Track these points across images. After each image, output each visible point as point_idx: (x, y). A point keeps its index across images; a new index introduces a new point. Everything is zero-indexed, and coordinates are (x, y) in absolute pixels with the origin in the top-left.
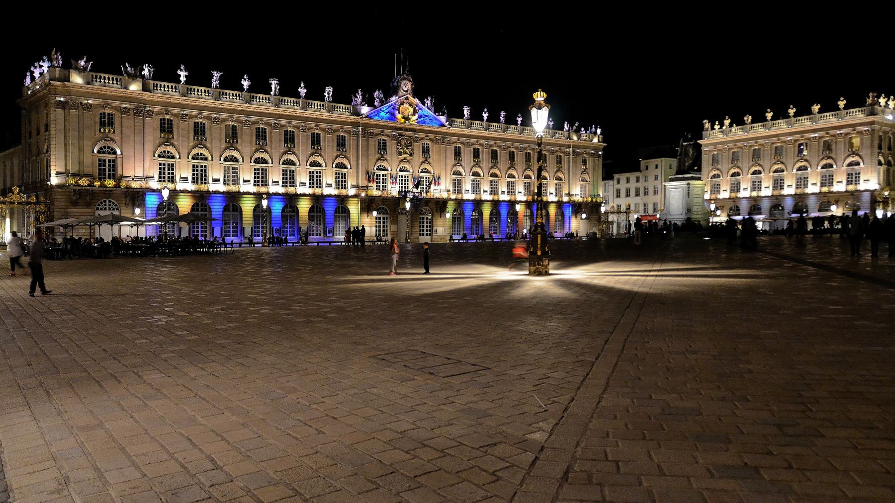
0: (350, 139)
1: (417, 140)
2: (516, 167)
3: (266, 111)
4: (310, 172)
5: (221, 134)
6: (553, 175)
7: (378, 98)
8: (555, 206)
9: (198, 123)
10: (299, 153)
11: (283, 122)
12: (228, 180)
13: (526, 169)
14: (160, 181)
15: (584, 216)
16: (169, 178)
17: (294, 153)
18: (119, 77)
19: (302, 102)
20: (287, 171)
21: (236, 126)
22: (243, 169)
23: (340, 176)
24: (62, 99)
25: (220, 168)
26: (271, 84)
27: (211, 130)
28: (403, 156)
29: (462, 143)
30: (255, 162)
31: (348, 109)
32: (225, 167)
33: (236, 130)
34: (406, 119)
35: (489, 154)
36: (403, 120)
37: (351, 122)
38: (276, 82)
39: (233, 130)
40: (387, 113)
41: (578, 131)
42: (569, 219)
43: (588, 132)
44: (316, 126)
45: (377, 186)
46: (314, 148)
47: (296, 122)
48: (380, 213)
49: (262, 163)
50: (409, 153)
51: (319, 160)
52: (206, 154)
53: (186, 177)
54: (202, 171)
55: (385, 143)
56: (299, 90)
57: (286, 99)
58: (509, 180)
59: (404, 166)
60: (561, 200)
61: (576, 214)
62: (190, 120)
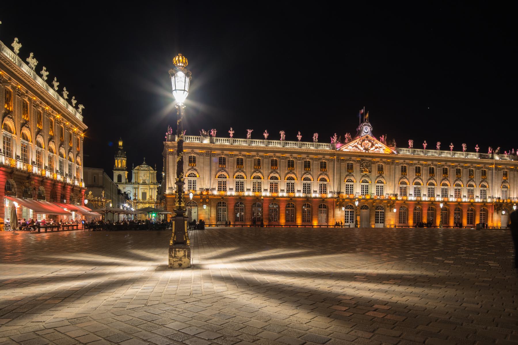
0: (329, 164)
1: (374, 163)
2: (449, 179)
3: (277, 150)
4: (304, 184)
5: (251, 164)
6: (479, 184)
7: (347, 138)
9: (239, 158)
10: (297, 173)
11: (287, 155)
12: (256, 189)
13: (456, 180)
14: (219, 191)
15: (504, 212)
16: (223, 189)
17: (294, 173)
18: (199, 137)
19: (299, 143)
20: (289, 184)
21: (260, 159)
22: (263, 183)
23: (323, 186)
24: (172, 150)
25: (251, 183)
26: (281, 134)
27: (246, 162)
28: (365, 173)
29: (407, 164)
30: (270, 179)
31: (328, 146)
32: (254, 183)
33: (260, 161)
35: (427, 171)
36: (364, 151)
37: (330, 154)
38: (283, 133)
39: (258, 161)
40: (353, 147)
41: (501, 152)
42: (492, 215)
43: (509, 154)
44: (307, 157)
45: (346, 192)
46: (306, 170)
48: (348, 209)
49: (275, 179)
50: (368, 171)
51: (309, 176)
52: (243, 175)
53: (232, 188)
54: (241, 185)
55: (352, 165)
56: (297, 136)
57: (289, 142)
58: (443, 187)
59: (365, 179)
60: (485, 201)
61: (498, 211)
62: (235, 157)
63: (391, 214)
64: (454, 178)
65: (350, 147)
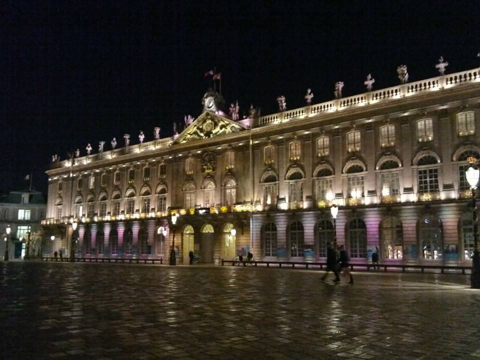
8: (138, 224)
34: (208, 134)
37: (169, 152)
50: (211, 167)
63: (245, 238)
65: (189, 136)
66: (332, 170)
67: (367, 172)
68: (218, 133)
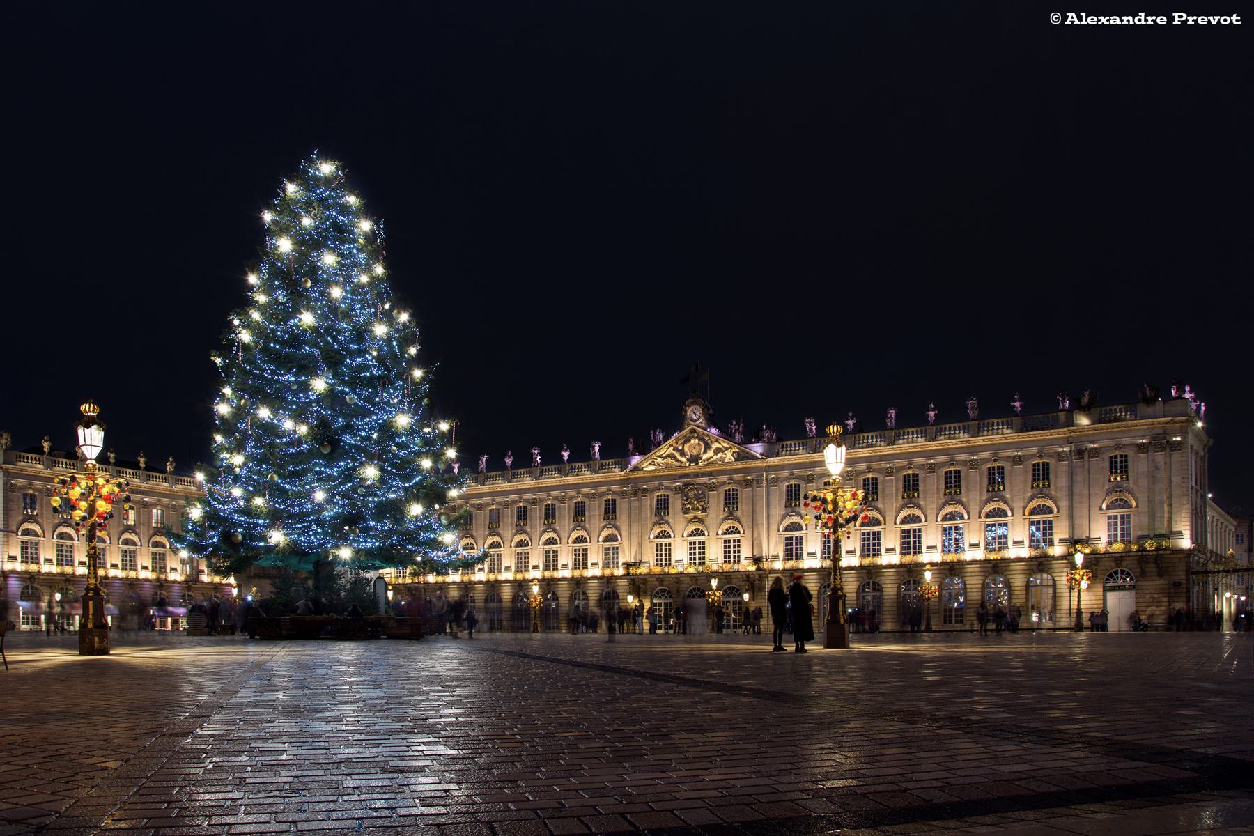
1: (713, 487)
6: (1022, 505)
11: (543, 495)
28: (692, 514)
34: (695, 459)
37: (621, 480)
38: (536, 452)
46: (578, 521)
47: (555, 493)
50: (700, 508)
64: (938, 498)
65: (659, 460)
66: (881, 519)
67: (926, 524)
68: (712, 460)
